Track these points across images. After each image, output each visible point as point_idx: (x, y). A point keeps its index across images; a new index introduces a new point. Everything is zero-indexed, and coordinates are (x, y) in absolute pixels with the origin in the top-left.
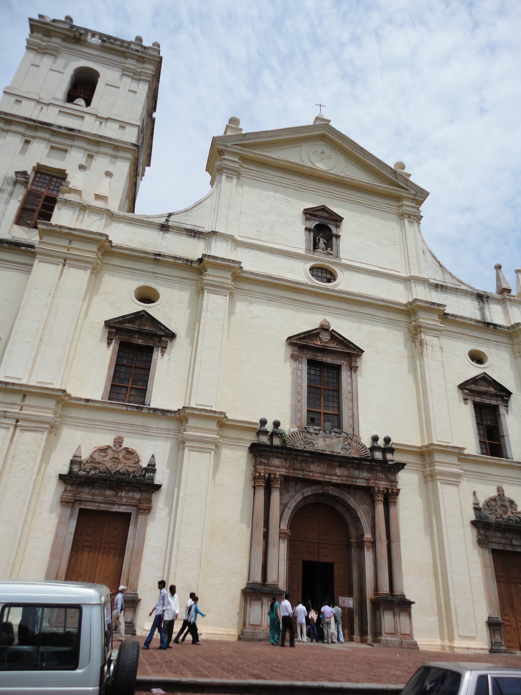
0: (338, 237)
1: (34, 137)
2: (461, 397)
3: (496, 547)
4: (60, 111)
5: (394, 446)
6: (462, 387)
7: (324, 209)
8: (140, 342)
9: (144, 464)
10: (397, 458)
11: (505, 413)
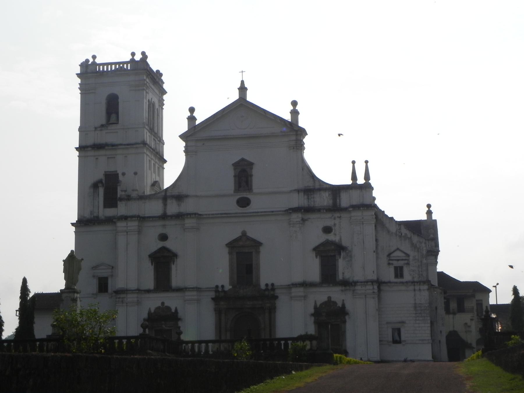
0: (251, 176)
1: (99, 156)
4: (106, 133)
5: (276, 287)
6: (315, 249)
7: (243, 160)
9: (173, 311)
10: (278, 292)
11: (339, 258)
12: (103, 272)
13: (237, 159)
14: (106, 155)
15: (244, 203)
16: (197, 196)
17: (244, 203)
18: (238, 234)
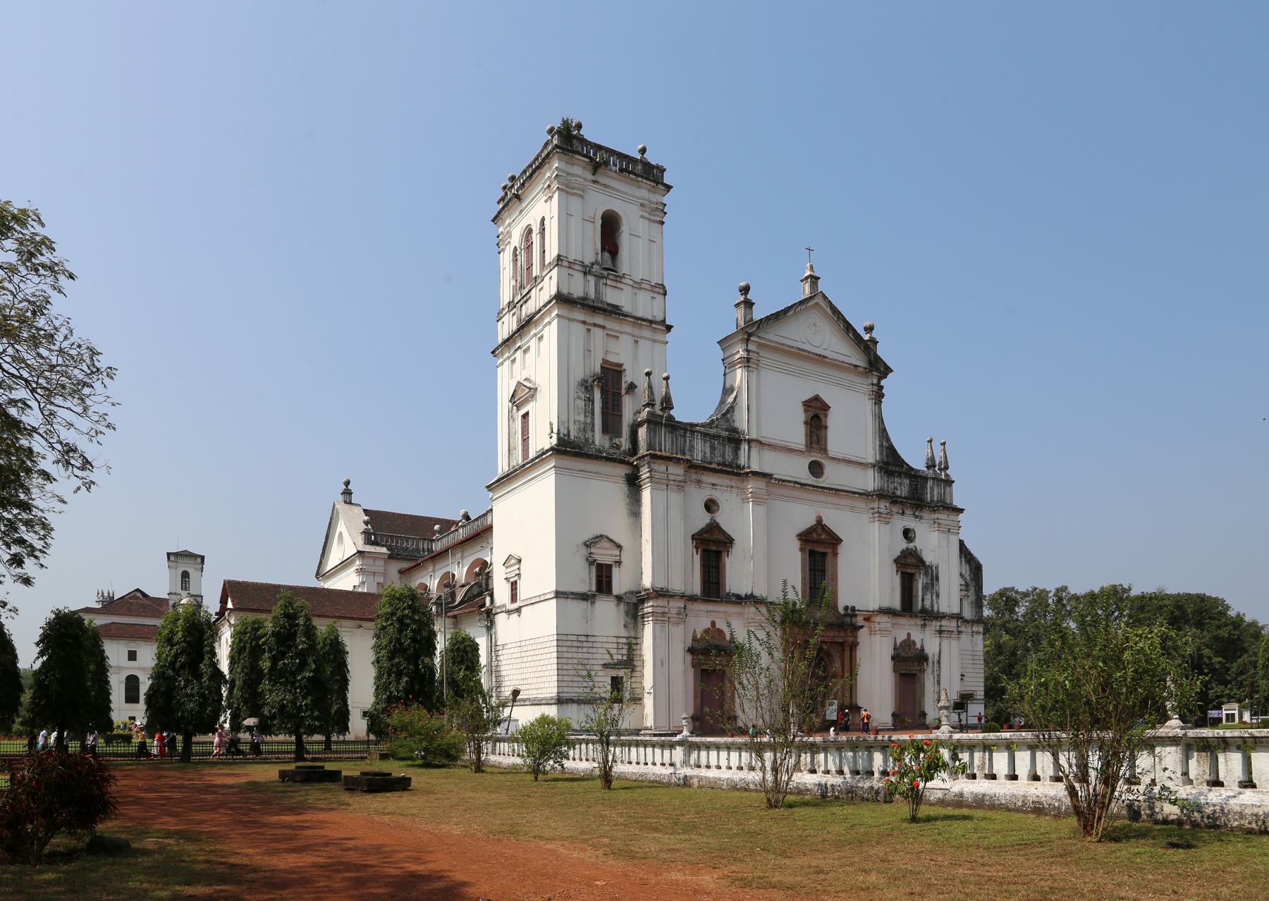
0: (826, 427)
2: (895, 569)
3: (902, 672)
8: (714, 548)
12: (604, 555)
13: (808, 395)
14: (604, 327)
15: (816, 469)
16: (760, 442)
17: (816, 469)
18: (811, 522)
